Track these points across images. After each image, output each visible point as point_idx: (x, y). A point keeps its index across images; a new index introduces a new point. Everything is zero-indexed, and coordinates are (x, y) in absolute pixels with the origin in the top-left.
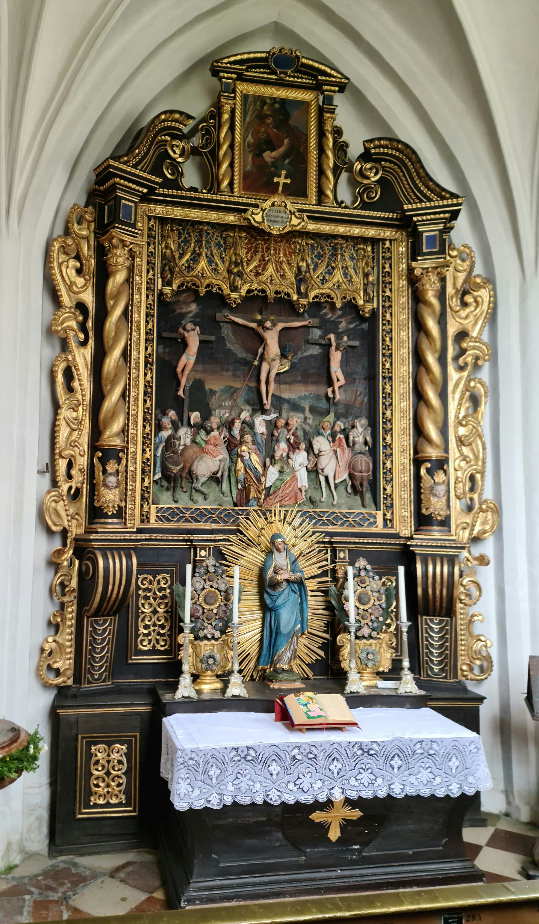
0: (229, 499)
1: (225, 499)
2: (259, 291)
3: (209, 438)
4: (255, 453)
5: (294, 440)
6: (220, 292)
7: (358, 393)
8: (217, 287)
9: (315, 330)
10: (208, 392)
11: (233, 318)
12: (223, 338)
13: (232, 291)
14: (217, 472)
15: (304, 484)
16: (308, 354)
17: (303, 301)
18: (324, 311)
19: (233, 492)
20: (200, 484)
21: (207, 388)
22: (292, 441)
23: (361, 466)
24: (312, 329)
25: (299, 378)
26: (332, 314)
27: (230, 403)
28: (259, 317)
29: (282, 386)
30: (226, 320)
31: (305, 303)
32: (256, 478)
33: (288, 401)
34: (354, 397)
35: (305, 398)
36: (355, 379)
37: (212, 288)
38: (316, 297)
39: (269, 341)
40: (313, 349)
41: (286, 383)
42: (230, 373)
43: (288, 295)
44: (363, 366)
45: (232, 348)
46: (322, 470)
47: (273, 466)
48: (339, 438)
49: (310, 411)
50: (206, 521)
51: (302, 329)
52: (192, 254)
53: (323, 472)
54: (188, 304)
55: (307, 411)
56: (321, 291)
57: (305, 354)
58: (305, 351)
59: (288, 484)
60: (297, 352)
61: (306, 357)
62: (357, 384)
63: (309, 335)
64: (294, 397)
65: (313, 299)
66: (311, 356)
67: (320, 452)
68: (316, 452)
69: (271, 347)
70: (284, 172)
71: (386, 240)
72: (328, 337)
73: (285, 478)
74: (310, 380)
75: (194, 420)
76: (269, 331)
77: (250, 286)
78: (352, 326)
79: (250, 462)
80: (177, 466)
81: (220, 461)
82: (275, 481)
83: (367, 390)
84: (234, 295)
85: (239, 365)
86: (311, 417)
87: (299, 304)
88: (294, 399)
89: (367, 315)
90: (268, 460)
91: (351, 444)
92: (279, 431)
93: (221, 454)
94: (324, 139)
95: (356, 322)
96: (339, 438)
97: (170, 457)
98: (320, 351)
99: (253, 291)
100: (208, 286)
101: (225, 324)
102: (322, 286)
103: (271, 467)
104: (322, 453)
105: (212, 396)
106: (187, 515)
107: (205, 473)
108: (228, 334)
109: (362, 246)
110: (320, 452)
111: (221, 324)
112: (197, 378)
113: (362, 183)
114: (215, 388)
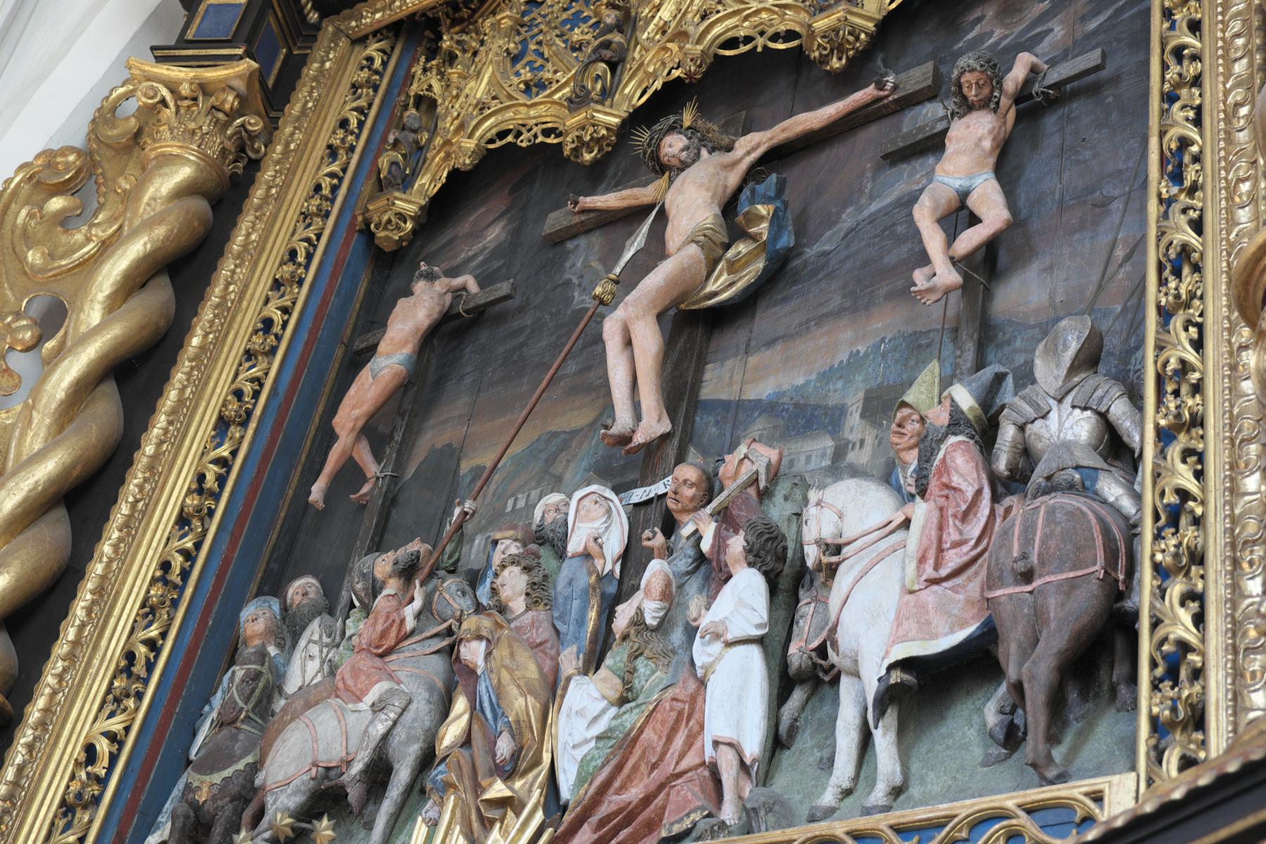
7: (1120, 253)
12: (568, 283)
15: (726, 733)
22: (706, 546)
23: (1027, 541)
25: (836, 301)
29: (753, 360)
33: (769, 407)
34: (1095, 277)
36: (1104, 204)
37: (519, 134)
40: (910, 176)
41: (770, 343)
43: (790, 35)
49: (863, 416)
55: (854, 419)
57: (874, 207)
58: (872, 198)
60: (839, 214)
61: (872, 219)
62: (1116, 218)
64: (800, 381)
68: (812, 554)
74: (883, 292)
78: (1093, 25)
81: (377, 708)
88: (797, 389)
90: (570, 660)
91: (1002, 465)
100: (502, 134)
108: (586, 266)
110: (838, 550)
111: (570, 245)
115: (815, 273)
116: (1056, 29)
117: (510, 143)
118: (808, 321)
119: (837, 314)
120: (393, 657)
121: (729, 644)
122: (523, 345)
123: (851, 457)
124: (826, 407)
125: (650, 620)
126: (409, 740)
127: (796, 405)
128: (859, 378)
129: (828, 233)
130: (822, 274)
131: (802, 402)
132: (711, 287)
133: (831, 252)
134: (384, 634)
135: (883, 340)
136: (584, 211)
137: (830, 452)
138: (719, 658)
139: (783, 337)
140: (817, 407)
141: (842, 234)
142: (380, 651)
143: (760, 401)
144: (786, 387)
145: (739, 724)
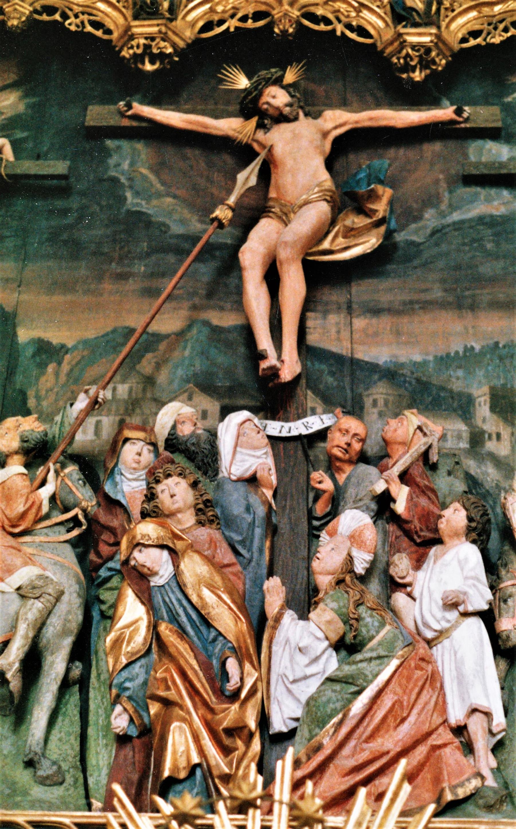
2: (244, 19)
4: (209, 560)
5: (410, 499)
6: (99, 33)
8: (85, 18)
10: (30, 351)
12: (115, 181)
13: (136, 17)
15: (481, 702)
19: (92, 760)
25: (437, 294)
29: (359, 323)
30: (126, 122)
31: (426, 39)
32: (206, 667)
37: (64, 16)
38: (475, 34)
42: (132, 285)
43: (362, 31)
45: (144, 207)
47: (303, 616)
49: (493, 408)
57: (456, 216)
58: (452, 208)
59: (387, 701)
61: (458, 226)
64: (418, 358)
65: (464, 40)
66: (481, 220)
73: (367, 668)
76: (285, 128)
77: (212, 10)
82: (319, 691)
86: (506, 432)
87: (403, 44)
88: (415, 364)
92: (341, 478)
93: (29, 560)
101: (125, 144)
103: (289, 616)
105: (42, 366)
115: (408, 259)
117: (56, 21)
118: (411, 302)
119: (443, 305)
120: (27, 539)
121: (466, 614)
122: (71, 227)
123: (491, 446)
124: (451, 391)
125: (360, 568)
126: (64, 633)
127: (418, 380)
128: (480, 373)
129: (413, 226)
130: (416, 262)
131: (424, 379)
132: (326, 245)
133: (419, 244)
134: (23, 516)
136: (137, 117)
137: (466, 435)
138: (454, 626)
140: (442, 388)
141: (429, 231)
142: (17, 530)
143: (377, 365)
144: (403, 359)
145: (487, 696)
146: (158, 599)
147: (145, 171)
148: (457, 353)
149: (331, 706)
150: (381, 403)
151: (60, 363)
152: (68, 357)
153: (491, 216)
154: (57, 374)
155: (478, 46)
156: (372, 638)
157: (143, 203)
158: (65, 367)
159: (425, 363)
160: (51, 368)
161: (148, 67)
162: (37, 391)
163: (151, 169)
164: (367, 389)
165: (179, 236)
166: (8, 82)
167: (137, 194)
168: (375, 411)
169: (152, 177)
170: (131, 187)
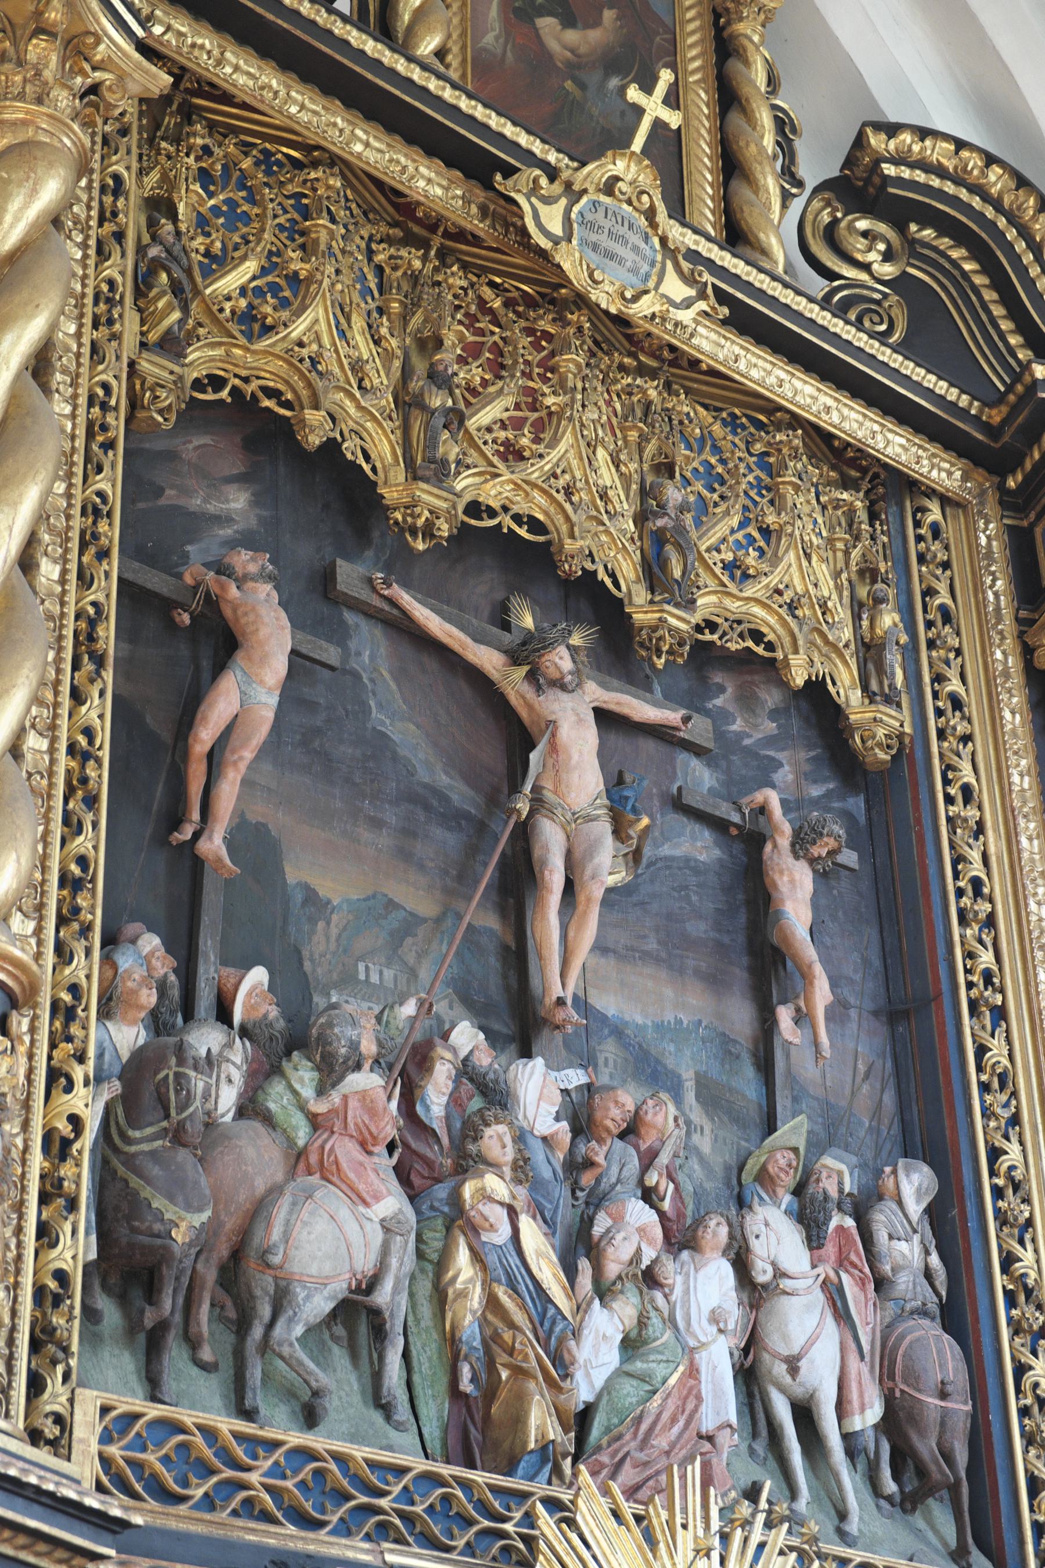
0: (411, 1439)
1: (393, 1434)
3: (335, 1097)
7: (862, 1068)
9: (695, 763)
10: (299, 897)
11: (406, 599)
12: (356, 676)
14: (372, 1284)
16: (678, 853)
17: (679, 621)
18: (719, 702)
19: (423, 1411)
20: (299, 1330)
21: (293, 875)
24: (682, 757)
26: (746, 721)
27: (389, 974)
28: (528, 621)
30: (377, 602)
34: (849, 1079)
35: (676, 1032)
39: (566, 732)
40: (694, 838)
44: (866, 961)
46: (793, 1365)
48: (840, 1229)
50: (345, 1529)
51: (649, 746)
52: (264, 271)
53: (794, 1370)
54: (216, 484)
55: (690, 1096)
56: (728, 602)
63: (673, 777)
64: (639, 1020)
67: (779, 1274)
69: (575, 757)
70: (634, 94)
71: (931, 493)
72: (759, 797)
73: (660, 1371)
75: (248, 1007)
79: (514, 1261)
80: (189, 1207)
83: (889, 1064)
84: (428, 495)
85: (421, 815)
89: (882, 756)
94: (734, 65)
95: (825, 780)
96: (840, 1229)
97: (153, 1154)
98: (717, 853)
99: (492, 513)
102: (732, 588)
104: (785, 1284)
105: (313, 921)
106: (254, 1478)
107: (327, 1268)
109: (845, 496)
111: (350, 618)
112: (252, 818)
113: (841, 277)
114: (327, 888)
116: (787, 768)
118: (633, 949)
119: (658, 960)
135: (700, 1022)
139: (614, 952)
144: (627, 1018)
146: (492, 1259)
147: (385, 673)
148: (669, 1022)
149: (629, 1399)
150: (611, 1063)
151: (328, 923)
152: (335, 917)
153: (696, 860)
154: (328, 938)
155: (713, 643)
156: (655, 1340)
157: (388, 722)
158: (334, 931)
159: (645, 1027)
160: (321, 925)
161: (420, 546)
162: (311, 955)
163: (391, 673)
164: (599, 1044)
165: (426, 786)
166: (235, 472)
167: (380, 706)
168: (607, 1071)
169: (393, 685)
170: (374, 694)
